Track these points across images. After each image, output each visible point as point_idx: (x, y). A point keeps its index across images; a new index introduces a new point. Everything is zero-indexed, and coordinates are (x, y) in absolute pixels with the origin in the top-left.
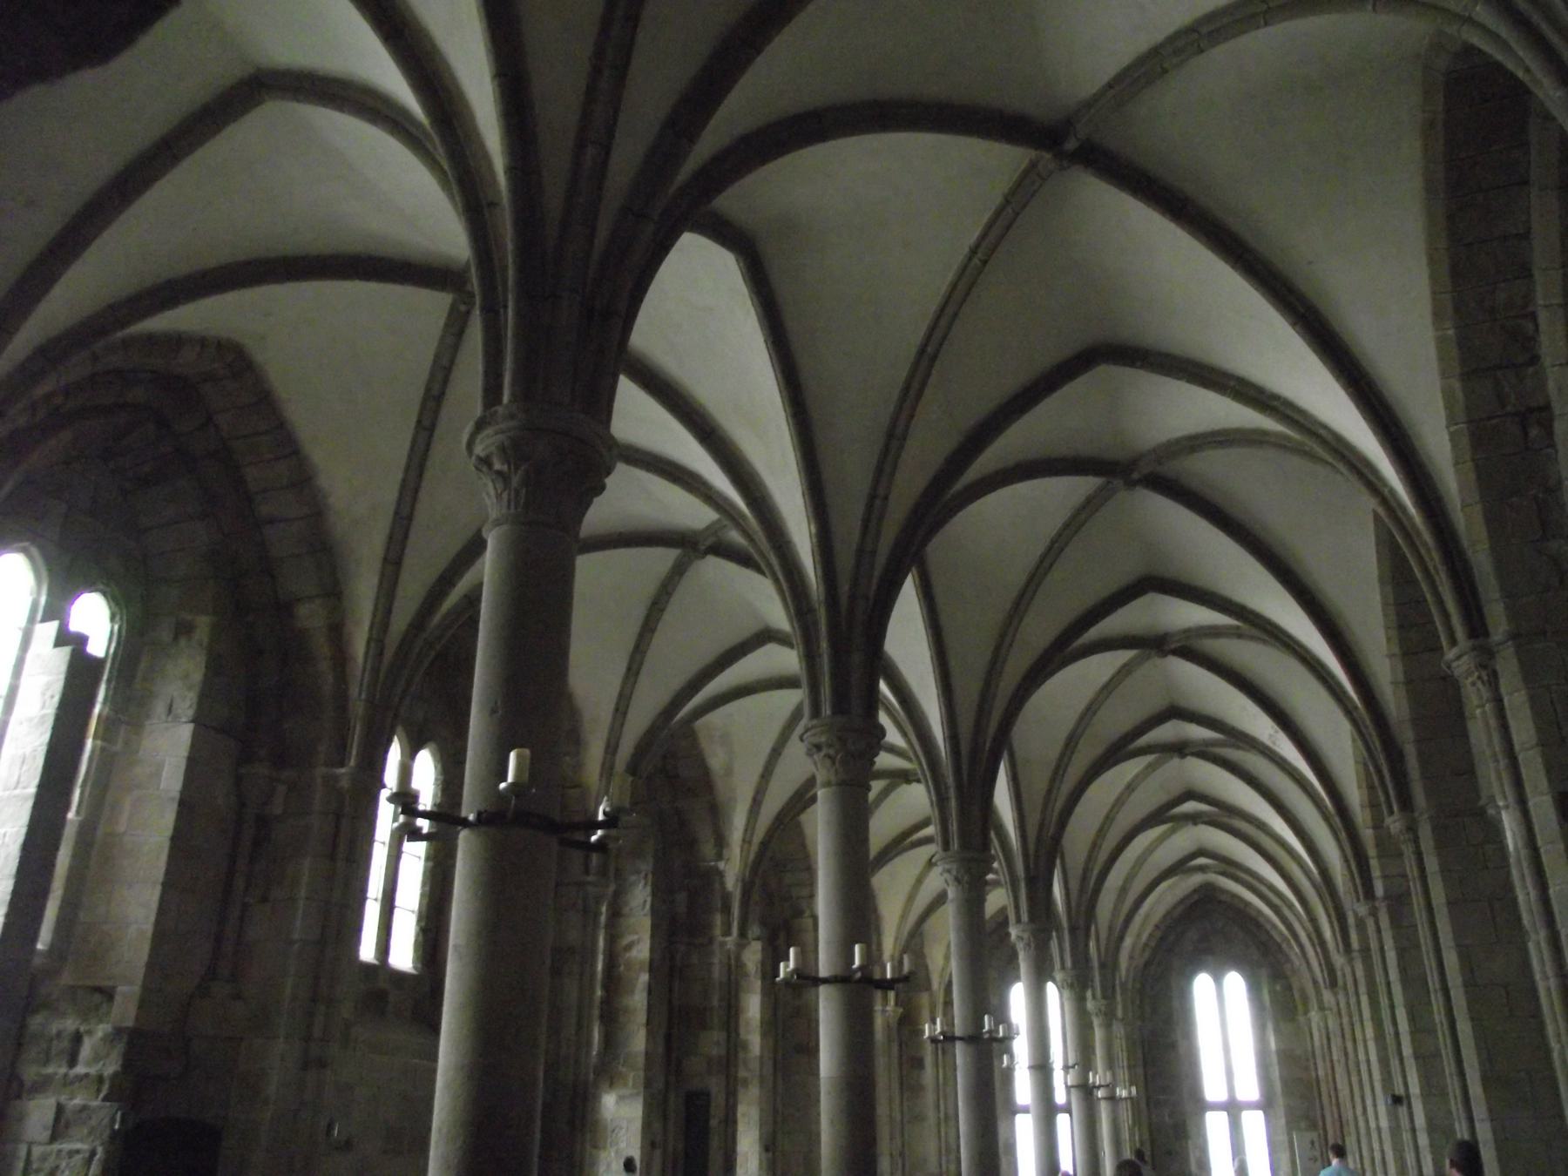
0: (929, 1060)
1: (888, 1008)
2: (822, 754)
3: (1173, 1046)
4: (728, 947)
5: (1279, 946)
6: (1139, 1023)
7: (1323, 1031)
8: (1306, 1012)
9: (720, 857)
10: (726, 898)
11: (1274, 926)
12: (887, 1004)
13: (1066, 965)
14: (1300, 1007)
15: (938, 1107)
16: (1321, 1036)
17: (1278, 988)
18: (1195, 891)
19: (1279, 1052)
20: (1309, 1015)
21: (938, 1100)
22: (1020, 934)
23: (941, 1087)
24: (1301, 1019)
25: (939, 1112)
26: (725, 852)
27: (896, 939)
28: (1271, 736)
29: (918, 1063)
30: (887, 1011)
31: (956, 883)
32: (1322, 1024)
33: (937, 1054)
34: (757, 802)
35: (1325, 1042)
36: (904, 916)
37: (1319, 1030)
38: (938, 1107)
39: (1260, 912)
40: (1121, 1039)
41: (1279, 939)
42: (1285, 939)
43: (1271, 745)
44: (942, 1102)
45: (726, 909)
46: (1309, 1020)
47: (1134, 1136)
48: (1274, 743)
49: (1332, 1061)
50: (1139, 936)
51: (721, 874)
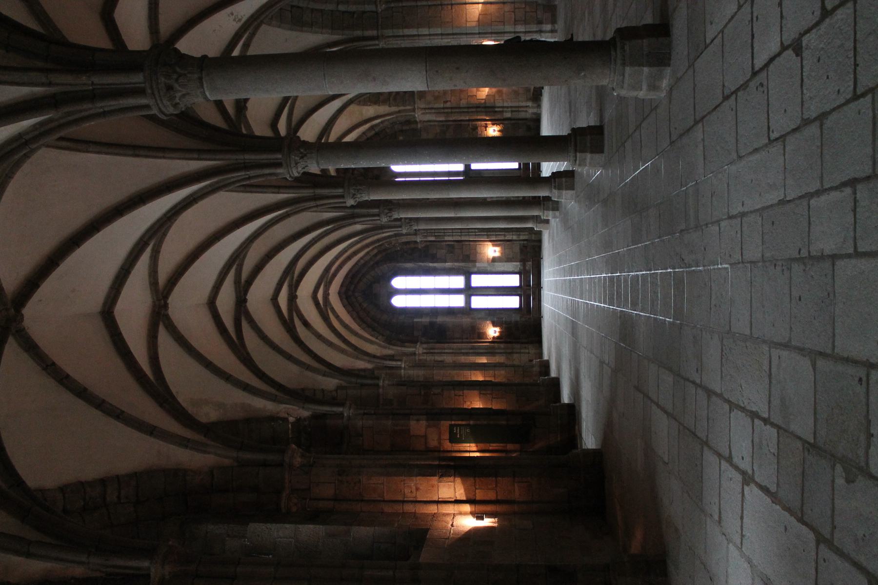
2: (176, 86)
4: (351, 414)
5: (377, 134)
8: (416, 122)
9: (285, 420)
10: (315, 417)
11: (364, 133)
12: (400, 367)
13: (378, 213)
14: (413, 126)
16: (430, 113)
21: (461, 353)
22: (351, 196)
23: (454, 351)
24: (419, 126)
25: (469, 353)
26: (283, 415)
27: (357, 358)
28: (234, 20)
31: (305, 158)
33: (435, 353)
34: (246, 387)
35: (433, 111)
36: (343, 351)
40: (428, 233)
41: (373, 132)
42: (372, 128)
43: (240, 24)
44: (463, 351)
45: (324, 416)
46: (420, 121)
48: (240, 20)
49: (444, 108)
51: (299, 420)
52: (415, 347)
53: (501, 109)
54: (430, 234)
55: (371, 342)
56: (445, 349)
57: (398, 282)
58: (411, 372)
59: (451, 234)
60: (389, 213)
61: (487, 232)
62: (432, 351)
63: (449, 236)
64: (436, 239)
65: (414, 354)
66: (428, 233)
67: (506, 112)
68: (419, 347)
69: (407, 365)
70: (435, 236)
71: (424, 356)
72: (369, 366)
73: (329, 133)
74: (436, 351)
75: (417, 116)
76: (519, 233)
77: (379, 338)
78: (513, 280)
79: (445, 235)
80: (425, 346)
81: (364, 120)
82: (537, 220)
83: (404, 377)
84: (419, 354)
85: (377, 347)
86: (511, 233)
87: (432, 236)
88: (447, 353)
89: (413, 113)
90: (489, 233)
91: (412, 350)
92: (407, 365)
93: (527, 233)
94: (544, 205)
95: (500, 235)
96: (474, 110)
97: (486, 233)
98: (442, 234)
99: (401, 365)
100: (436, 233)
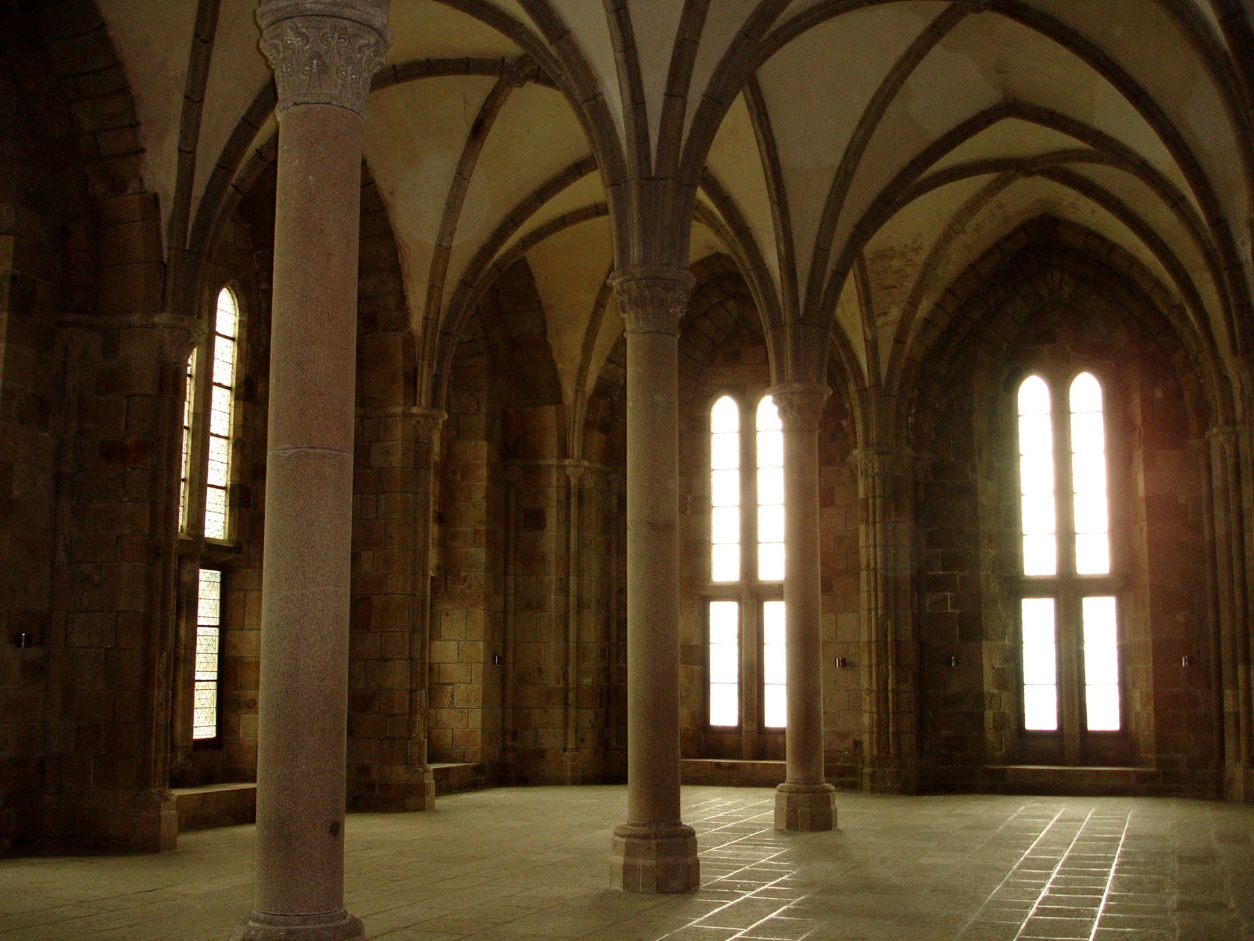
0: (552, 517)
1: (414, 410)
3: (969, 491)
6: (908, 451)
7: (1230, 461)
11: (1158, 284)
15: (565, 590)
16: (1225, 469)
17: (1159, 394)
18: (1023, 228)
19: (1148, 499)
20: (1207, 434)
29: (536, 520)
30: (412, 415)
32: (1229, 450)
35: (1231, 478)
37: (1224, 460)
38: (565, 590)
39: (1133, 260)
40: (874, 477)
46: (1208, 444)
47: (885, 635)
50: (913, 304)
52: (584, 456)
53: (1241, 683)
54: (871, 484)
55: (587, 348)
56: (579, 531)
57: (768, 411)
58: (398, 432)
59: (871, 541)
60: (630, 298)
61: (877, 641)
62: (573, 500)
63: (867, 535)
64: (861, 500)
65: (564, 453)
66: (874, 477)
67: (1235, 697)
68: (586, 468)
69: (418, 422)
70: (867, 499)
71: (558, 480)
72: (416, 323)
73: (1100, 160)
74: (573, 510)
75: (1215, 431)
76: (875, 729)
77: (611, 365)
78: (777, 714)
79: (867, 523)
80: (590, 482)
81: (1188, 277)
82: (797, 792)
83: (387, 416)
84: (564, 468)
85: (578, 361)
86: (874, 710)
87: (866, 492)
88: (568, 540)
89: (1220, 422)
90: (873, 646)
91: (575, 447)
92: (418, 422)
93: (875, 752)
94: (646, 837)
95: (871, 680)
96: (1238, 603)
97: (874, 639)
98: (871, 517)
99: (420, 405)
100: (874, 502)
